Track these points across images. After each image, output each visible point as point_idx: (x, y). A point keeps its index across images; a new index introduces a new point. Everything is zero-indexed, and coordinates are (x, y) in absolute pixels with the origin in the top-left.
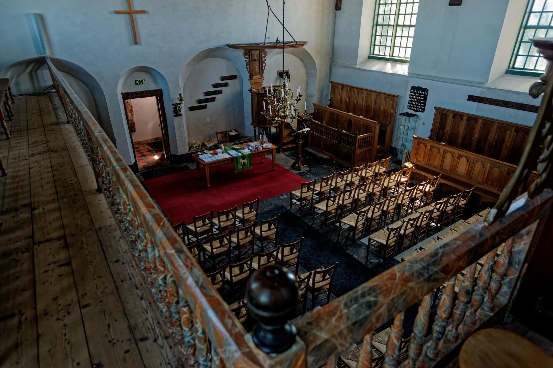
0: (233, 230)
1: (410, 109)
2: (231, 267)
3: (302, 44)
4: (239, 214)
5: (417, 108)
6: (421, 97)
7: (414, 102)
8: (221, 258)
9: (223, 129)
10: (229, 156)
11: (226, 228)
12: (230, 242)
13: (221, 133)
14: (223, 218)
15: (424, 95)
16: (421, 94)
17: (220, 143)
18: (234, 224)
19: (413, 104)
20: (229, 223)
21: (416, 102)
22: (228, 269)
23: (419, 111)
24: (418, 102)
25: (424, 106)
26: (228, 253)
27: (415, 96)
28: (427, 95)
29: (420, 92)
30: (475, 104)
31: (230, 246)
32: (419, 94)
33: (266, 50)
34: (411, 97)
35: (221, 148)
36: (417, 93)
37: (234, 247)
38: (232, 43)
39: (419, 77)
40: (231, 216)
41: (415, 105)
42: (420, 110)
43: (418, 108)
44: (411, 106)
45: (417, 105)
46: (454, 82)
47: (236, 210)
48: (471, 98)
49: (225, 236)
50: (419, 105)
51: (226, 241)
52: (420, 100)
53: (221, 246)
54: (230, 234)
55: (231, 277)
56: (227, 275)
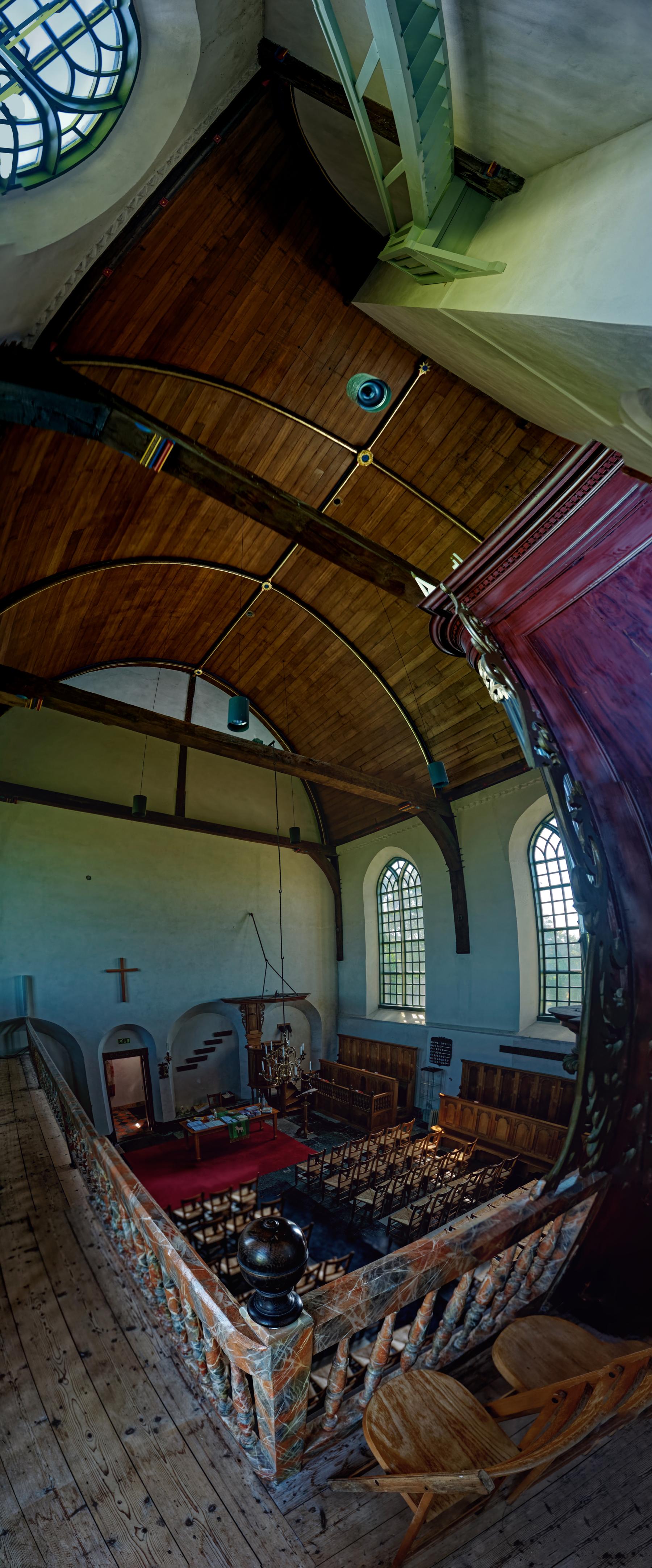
0: (228, 1215)
2: (228, 1258)
3: (305, 995)
4: (236, 1197)
8: (215, 1249)
9: (216, 1092)
10: (222, 1124)
11: (219, 1214)
12: (225, 1229)
13: (213, 1096)
14: (217, 1201)
17: (212, 1107)
18: (230, 1209)
20: (224, 1207)
22: (224, 1261)
26: (223, 1242)
31: (226, 1235)
33: (265, 1004)
35: (213, 1114)
37: (231, 1236)
38: (227, 997)
40: (226, 1199)
47: (231, 1191)
49: (220, 1222)
51: (220, 1229)
53: (216, 1234)
54: (225, 1220)
55: (228, 1269)
56: (224, 1267)
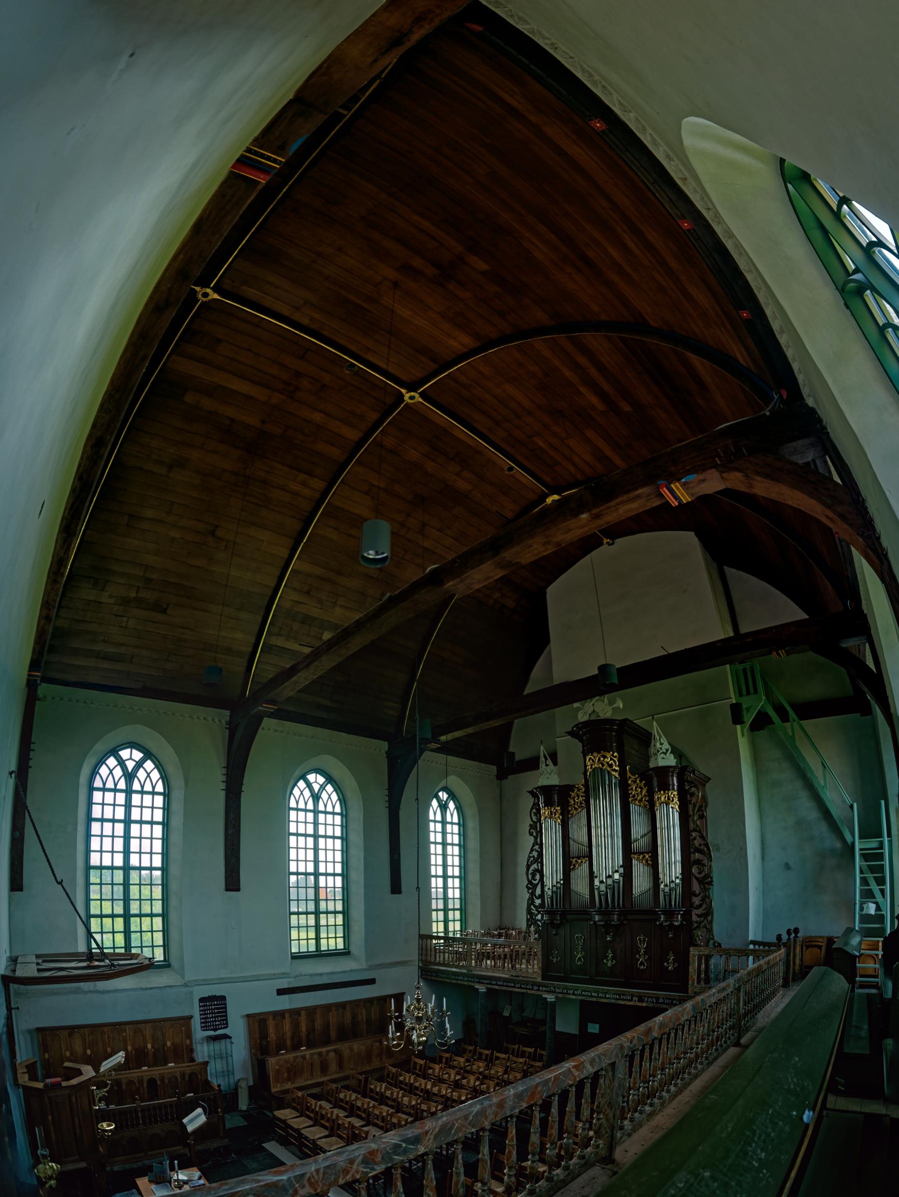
1: (207, 1030)
5: (216, 1025)
6: (217, 1009)
7: (210, 1018)
15: (222, 1004)
16: (217, 1005)
19: (208, 1022)
21: (212, 1017)
23: (222, 1028)
24: (215, 1017)
25: (226, 1020)
27: (209, 1009)
28: (225, 1004)
29: (216, 1003)
30: (286, 997)
32: (215, 1005)
34: (203, 1013)
36: (211, 1005)
39: (207, 983)
41: (213, 1021)
42: (223, 1026)
43: (218, 1025)
44: (206, 1026)
45: (215, 1021)
46: (257, 978)
48: (280, 992)
50: (218, 1021)
52: (218, 1013)
